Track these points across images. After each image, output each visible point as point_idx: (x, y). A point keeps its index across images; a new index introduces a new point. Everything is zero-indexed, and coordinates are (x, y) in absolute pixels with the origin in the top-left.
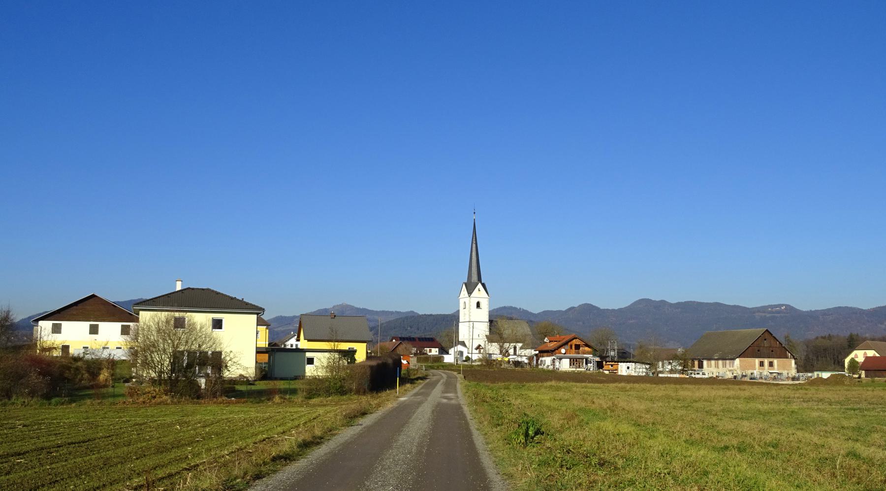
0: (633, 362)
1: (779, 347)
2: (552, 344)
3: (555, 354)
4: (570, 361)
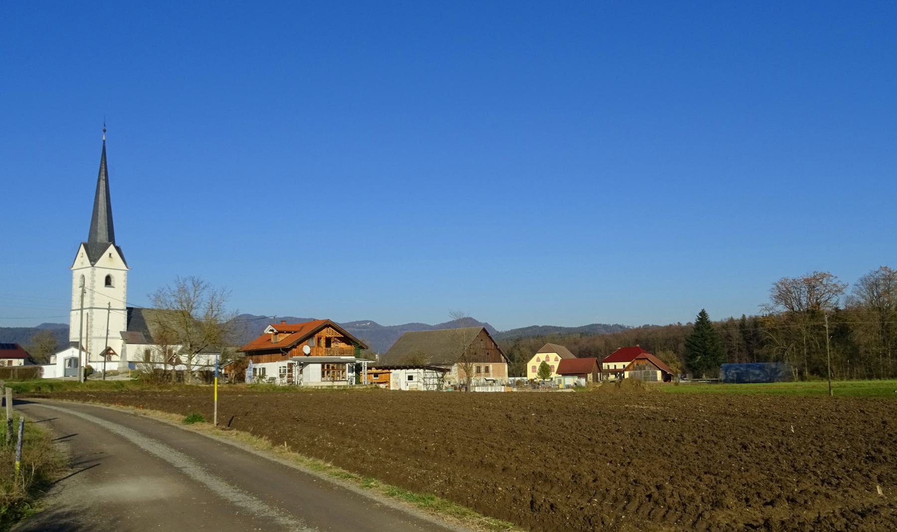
0: (420, 368)
1: (494, 349)
2: (281, 338)
3: (292, 356)
4: (323, 367)
